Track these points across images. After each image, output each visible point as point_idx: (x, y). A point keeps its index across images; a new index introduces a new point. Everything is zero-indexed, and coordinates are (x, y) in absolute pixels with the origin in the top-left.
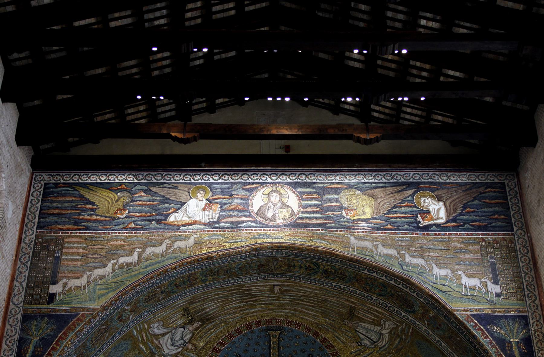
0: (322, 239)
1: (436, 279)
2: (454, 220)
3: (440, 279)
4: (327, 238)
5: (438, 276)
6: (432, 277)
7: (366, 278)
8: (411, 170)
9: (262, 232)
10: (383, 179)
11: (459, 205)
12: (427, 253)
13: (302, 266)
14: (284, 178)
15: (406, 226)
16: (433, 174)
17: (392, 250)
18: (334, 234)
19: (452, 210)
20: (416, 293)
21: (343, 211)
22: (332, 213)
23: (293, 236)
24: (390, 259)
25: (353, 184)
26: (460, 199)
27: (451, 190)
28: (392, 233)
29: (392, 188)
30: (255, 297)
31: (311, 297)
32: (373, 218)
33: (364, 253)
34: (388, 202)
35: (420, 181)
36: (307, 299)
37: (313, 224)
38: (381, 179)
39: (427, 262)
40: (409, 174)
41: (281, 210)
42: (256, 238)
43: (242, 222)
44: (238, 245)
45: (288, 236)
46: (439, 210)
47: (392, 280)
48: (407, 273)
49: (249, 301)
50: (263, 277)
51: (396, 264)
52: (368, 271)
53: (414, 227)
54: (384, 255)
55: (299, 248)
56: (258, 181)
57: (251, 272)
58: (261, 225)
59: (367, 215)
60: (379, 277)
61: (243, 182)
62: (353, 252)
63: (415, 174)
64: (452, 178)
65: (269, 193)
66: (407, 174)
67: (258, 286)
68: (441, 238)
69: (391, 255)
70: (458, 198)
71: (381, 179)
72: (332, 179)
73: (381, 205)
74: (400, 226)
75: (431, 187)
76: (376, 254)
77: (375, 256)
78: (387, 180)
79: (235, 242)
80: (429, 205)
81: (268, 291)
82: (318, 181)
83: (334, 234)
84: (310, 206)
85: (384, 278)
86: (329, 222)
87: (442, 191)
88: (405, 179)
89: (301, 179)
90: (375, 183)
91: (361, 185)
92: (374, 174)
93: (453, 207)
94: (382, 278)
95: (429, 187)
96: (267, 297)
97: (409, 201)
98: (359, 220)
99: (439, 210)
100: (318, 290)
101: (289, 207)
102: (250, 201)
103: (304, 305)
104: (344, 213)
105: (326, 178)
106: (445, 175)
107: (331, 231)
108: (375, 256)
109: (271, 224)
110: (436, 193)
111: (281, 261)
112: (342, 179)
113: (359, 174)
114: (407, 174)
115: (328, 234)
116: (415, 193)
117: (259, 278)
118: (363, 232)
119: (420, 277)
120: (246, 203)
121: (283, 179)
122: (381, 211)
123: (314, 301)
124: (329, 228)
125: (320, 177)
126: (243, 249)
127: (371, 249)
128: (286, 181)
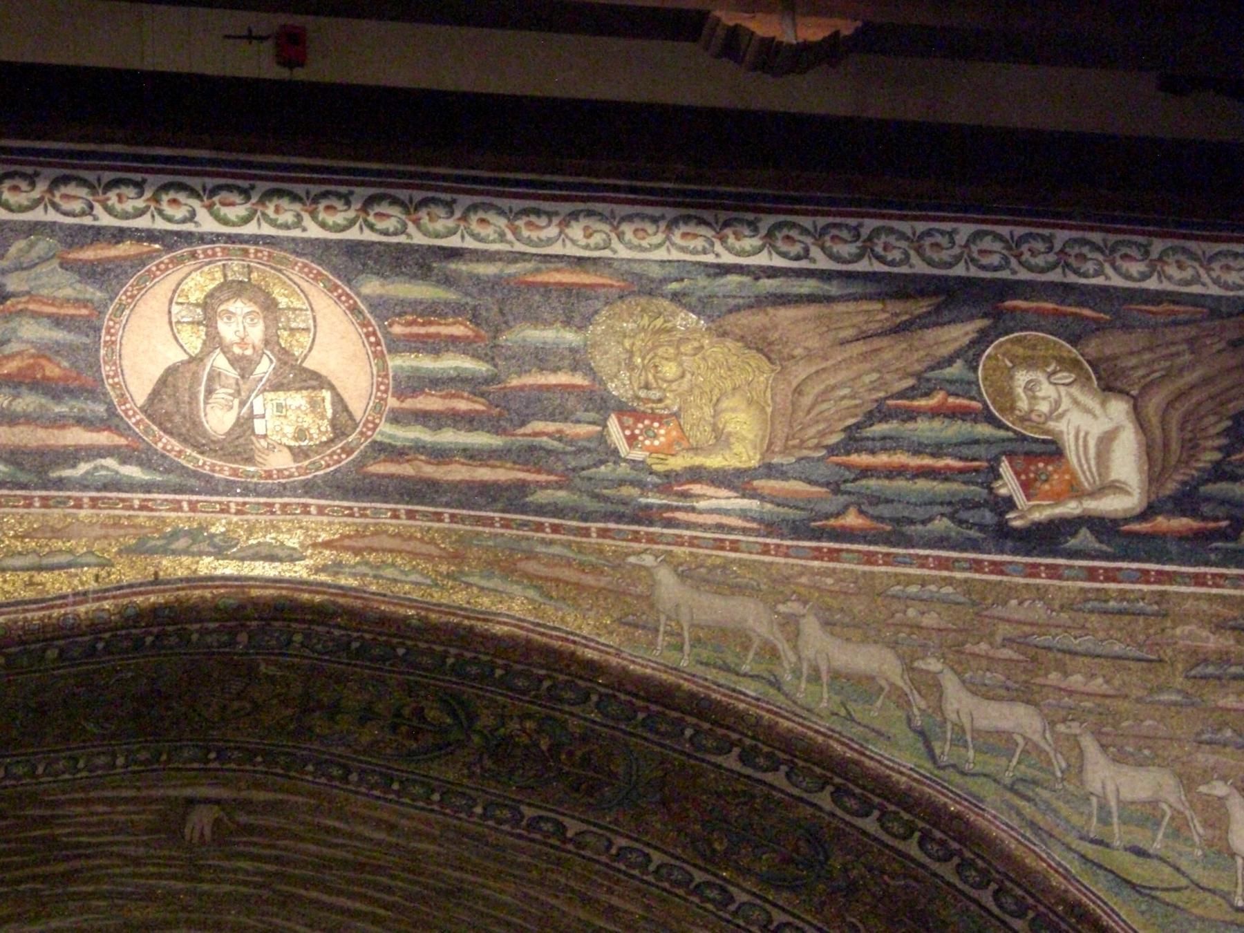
0: (509, 570)
1: (1105, 820)
2: (1185, 502)
3: (1124, 822)
4: (531, 566)
5: (1113, 803)
6: (1085, 809)
7: (719, 795)
8: (965, 209)
9: (182, 519)
10: (815, 252)
11: (1212, 419)
12: (1054, 677)
13: (380, 707)
14: (289, 217)
15: (941, 525)
16: (1075, 241)
17: (874, 650)
18: (568, 545)
19: (1175, 446)
20: (993, 886)
21: (613, 424)
22: (551, 427)
23: (357, 551)
24: (869, 698)
25: (656, 272)
26: (1213, 390)
27: (1169, 334)
28: (870, 559)
29: (866, 306)
30: (67, 859)
31: (378, 869)
32: (769, 470)
33: (731, 660)
34: (842, 385)
35: (1005, 274)
36: (350, 882)
37: (455, 486)
38: (806, 255)
39: (1053, 724)
40: (951, 234)
41: (281, 396)
42: (152, 551)
43: (73, 456)
44: (55, 583)
45: (327, 545)
46: (1107, 440)
47: (867, 815)
48: (957, 778)
49: (34, 878)
50: (143, 755)
51: (899, 730)
52: (742, 759)
53: (982, 527)
54: (836, 675)
55: (384, 620)
56: (143, 223)
57: (90, 727)
58: (173, 478)
59: (738, 448)
60: (796, 792)
61: (61, 226)
62: (677, 655)
63: (977, 236)
64: (1172, 270)
65: (211, 295)
66: (942, 233)
67: (103, 801)
68: (1122, 595)
69: (872, 679)
70: (1206, 381)
71: (807, 250)
72: (544, 234)
73: (806, 401)
74: (912, 522)
75: (1065, 315)
76: (797, 672)
77: (788, 677)
78: (837, 258)
79: (40, 568)
80: (1056, 413)
81: (148, 831)
82: (470, 243)
83: (568, 545)
84: (435, 382)
85: (824, 799)
86: (543, 478)
87: (1126, 337)
88: (930, 263)
89: (380, 225)
90: (772, 272)
91: (702, 281)
92: (768, 221)
93: (1182, 429)
94: (814, 798)
95: (1056, 313)
96: (137, 862)
97: (951, 382)
98: (696, 474)
99: (1107, 440)
100: (433, 839)
101: (314, 381)
102: (105, 337)
103: (331, 908)
104: (615, 432)
105: (515, 232)
106: (1133, 252)
107: (555, 529)
108: (788, 677)
109: (226, 475)
110: (1093, 347)
111: (272, 679)
112: (597, 238)
113: (687, 219)
114: (942, 233)
115: (540, 549)
116: (983, 339)
117: (120, 761)
118: (719, 545)
119: (1022, 803)
120: (85, 347)
121: (282, 219)
122: (812, 431)
123: (389, 890)
124: (540, 510)
125: (482, 221)
126: (82, 609)
127: (766, 642)
128: (296, 233)
